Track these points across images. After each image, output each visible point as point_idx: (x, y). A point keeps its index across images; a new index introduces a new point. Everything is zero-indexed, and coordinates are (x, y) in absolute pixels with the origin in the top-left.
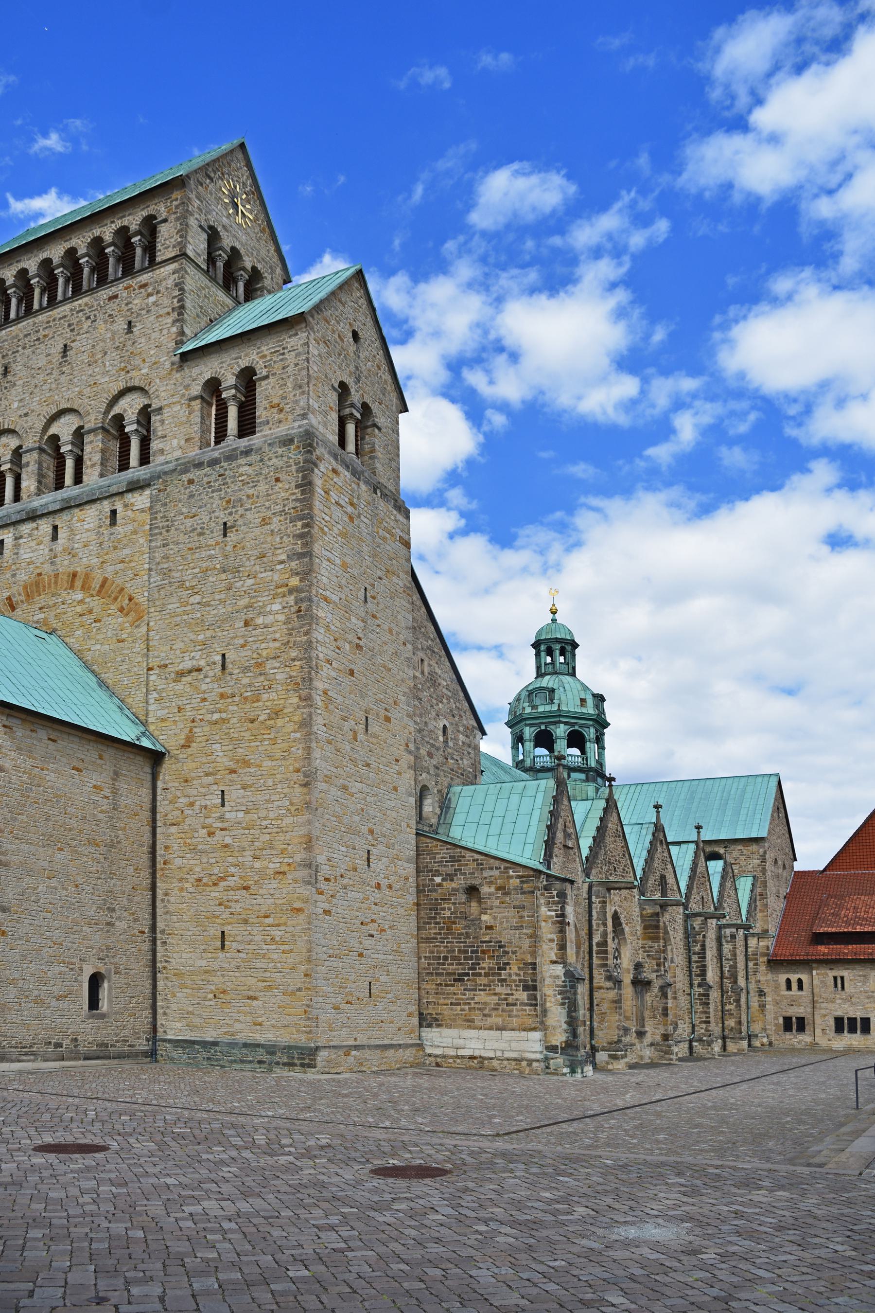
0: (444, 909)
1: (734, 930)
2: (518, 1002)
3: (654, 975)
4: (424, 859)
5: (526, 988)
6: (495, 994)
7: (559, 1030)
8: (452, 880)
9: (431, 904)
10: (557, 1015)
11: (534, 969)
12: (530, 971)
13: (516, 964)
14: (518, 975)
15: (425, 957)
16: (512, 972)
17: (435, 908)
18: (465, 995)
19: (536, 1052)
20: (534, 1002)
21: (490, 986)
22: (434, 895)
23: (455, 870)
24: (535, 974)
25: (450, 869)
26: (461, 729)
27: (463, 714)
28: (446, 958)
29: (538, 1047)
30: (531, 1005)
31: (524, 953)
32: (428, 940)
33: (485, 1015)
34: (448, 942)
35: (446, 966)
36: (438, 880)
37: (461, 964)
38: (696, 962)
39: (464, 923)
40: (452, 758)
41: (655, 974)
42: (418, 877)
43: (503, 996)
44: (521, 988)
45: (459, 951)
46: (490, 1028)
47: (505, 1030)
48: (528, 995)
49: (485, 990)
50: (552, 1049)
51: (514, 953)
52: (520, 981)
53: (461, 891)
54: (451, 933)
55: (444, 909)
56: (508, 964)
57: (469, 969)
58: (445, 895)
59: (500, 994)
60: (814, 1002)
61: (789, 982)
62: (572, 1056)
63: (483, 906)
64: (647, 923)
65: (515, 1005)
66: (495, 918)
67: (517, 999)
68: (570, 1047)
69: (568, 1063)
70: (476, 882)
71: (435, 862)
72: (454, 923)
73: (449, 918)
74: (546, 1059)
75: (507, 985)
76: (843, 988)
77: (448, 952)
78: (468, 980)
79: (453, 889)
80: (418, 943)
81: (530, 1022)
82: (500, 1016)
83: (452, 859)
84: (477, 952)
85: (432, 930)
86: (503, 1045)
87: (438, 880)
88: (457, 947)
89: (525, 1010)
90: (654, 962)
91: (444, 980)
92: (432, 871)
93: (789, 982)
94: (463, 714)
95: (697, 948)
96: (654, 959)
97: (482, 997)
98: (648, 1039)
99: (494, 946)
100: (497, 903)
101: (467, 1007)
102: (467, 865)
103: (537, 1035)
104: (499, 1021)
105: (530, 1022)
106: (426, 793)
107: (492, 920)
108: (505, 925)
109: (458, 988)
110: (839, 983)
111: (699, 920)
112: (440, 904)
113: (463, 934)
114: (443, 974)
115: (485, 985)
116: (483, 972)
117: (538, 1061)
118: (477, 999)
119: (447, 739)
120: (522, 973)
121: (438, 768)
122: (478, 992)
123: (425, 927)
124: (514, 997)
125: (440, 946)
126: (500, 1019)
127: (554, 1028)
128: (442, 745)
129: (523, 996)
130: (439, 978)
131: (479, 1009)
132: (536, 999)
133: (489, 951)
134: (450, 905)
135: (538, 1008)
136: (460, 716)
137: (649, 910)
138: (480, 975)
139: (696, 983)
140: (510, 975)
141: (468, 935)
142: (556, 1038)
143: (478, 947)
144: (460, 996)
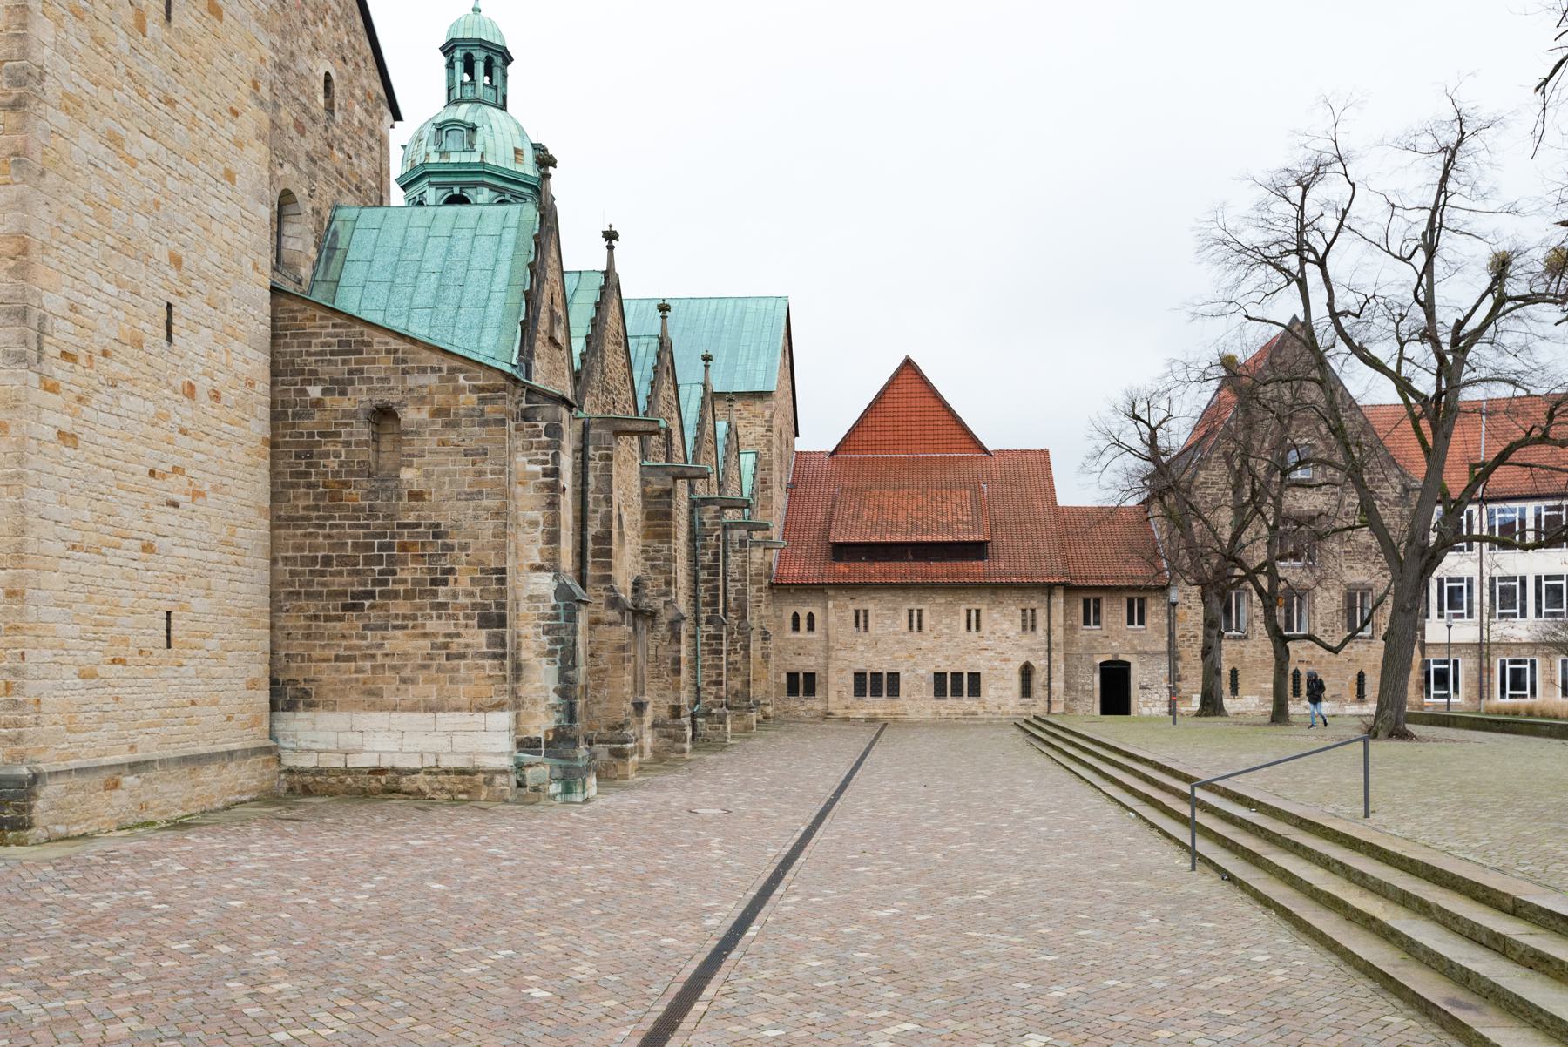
0: (326, 455)
1: (745, 532)
2: (470, 651)
3: (660, 602)
4: (287, 345)
5: (485, 621)
6: (425, 635)
7: (542, 707)
8: (343, 393)
9: (299, 444)
10: (542, 678)
11: (502, 581)
12: (495, 587)
13: (468, 571)
14: (471, 594)
15: (286, 558)
16: (459, 588)
17: (307, 454)
18: (364, 638)
19: (501, 754)
20: (499, 650)
21: (415, 618)
22: (305, 425)
23: (350, 372)
24: (502, 593)
25: (339, 370)
26: (358, 92)
27: (362, 64)
28: (327, 561)
29: (506, 743)
30: (494, 656)
31: (483, 548)
32: (292, 521)
33: (404, 681)
34: (332, 526)
35: (328, 578)
36: (315, 392)
37: (358, 573)
38: (706, 581)
39: (367, 484)
40: (341, 149)
41: (663, 599)
42: (273, 384)
43: (441, 640)
44: (475, 622)
45: (356, 546)
46: (414, 708)
47: (442, 709)
48: (489, 637)
49: (405, 627)
50: (527, 744)
51: (464, 548)
52: (475, 606)
53: (362, 416)
54: (339, 508)
55: (326, 455)
56: (451, 571)
57: (376, 582)
58: (329, 424)
59: (434, 635)
60: (828, 649)
61: (796, 618)
62: (568, 759)
63: (406, 449)
64: (652, 508)
65: (462, 656)
66: (428, 475)
67: (467, 646)
68: (561, 740)
69: (558, 773)
70: (393, 399)
71: (309, 354)
72: (346, 485)
73: (336, 474)
74: (520, 766)
75: (449, 616)
76: (866, 627)
77: (332, 547)
78: (372, 607)
79: (346, 414)
80: (273, 528)
81: (490, 692)
82: (434, 681)
83: (345, 348)
84: (390, 547)
85: (301, 501)
86: (440, 743)
87: (315, 392)
88: (350, 536)
89: (483, 667)
90: (661, 578)
91: (324, 608)
92: (302, 372)
93: (796, 618)
94: (362, 64)
95: (707, 559)
96: (661, 572)
97: (399, 641)
98: (648, 717)
99: (425, 535)
100: (433, 443)
101: (368, 664)
102: (373, 361)
103: (504, 719)
104: (431, 692)
105: (490, 692)
106: (289, 209)
107: (422, 480)
108: (447, 489)
109: (351, 624)
110: (861, 620)
111: (713, 508)
112: (319, 444)
113: (362, 509)
114: (320, 594)
115: (405, 617)
116: (401, 588)
117: (504, 772)
118: (388, 648)
119: (332, 105)
120: (477, 590)
121: (315, 162)
122: (391, 632)
123: (286, 495)
124: (461, 640)
125: (316, 536)
126: (434, 687)
127: (535, 703)
128: (323, 114)
129: (478, 638)
130: (311, 603)
131: (393, 668)
132: (504, 645)
133: (414, 544)
134: (339, 448)
135: (507, 662)
136: (357, 64)
137: (657, 485)
138: (396, 594)
139: (703, 616)
140: (455, 595)
141: (372, 512)
142: (537, 722)
143: (393, 536)
144: (355, 642)
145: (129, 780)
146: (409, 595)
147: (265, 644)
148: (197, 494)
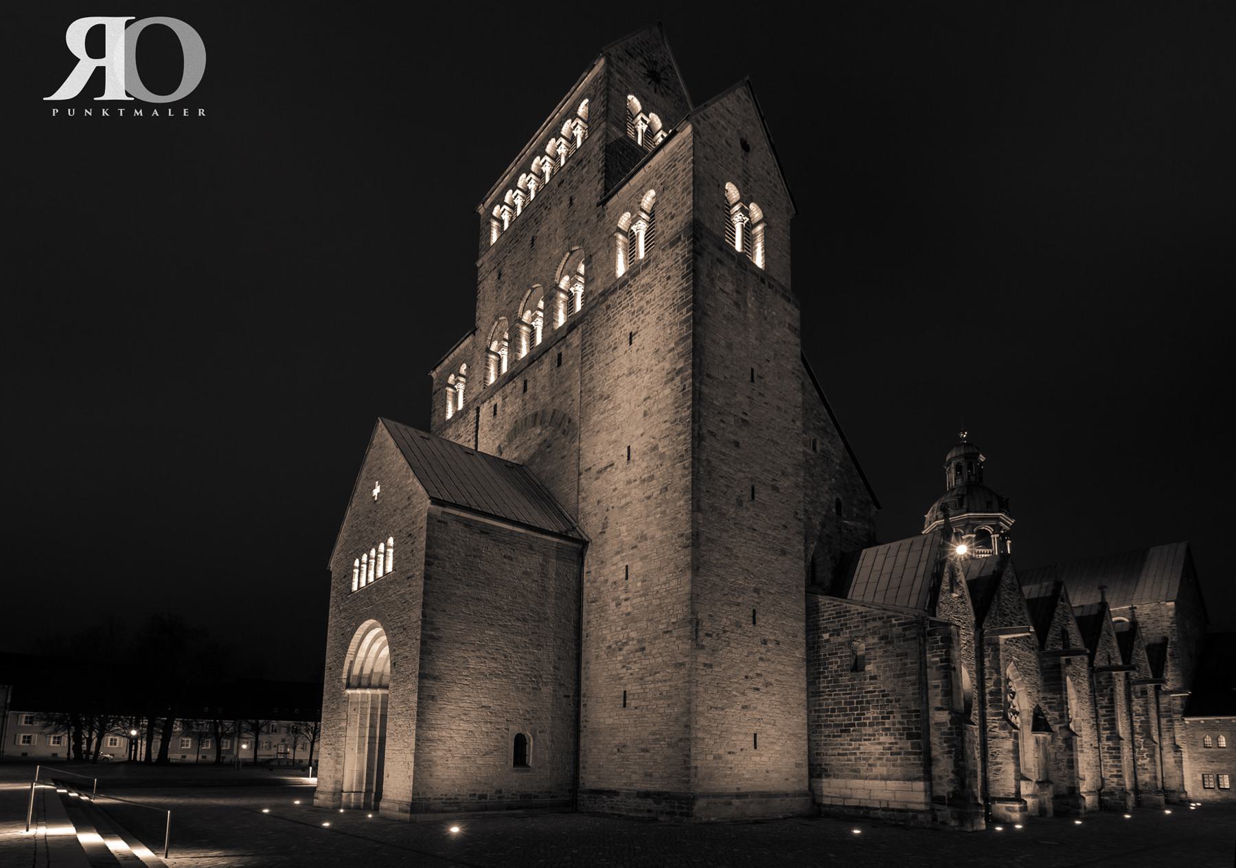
0: (831, 663)
25: (836, 625)
28: (833, 710)
29: (921, 797)
46: (875, 778)
56: (892, 712)
74: (932, 810)
79: (841, 644)
84: (861, 702)
87: (826, 636)
109: (845, 739)
138: (865, 724)
145: (736, 802)
146: (871, 725)
147: (806, 748)
148: (767, 684)
